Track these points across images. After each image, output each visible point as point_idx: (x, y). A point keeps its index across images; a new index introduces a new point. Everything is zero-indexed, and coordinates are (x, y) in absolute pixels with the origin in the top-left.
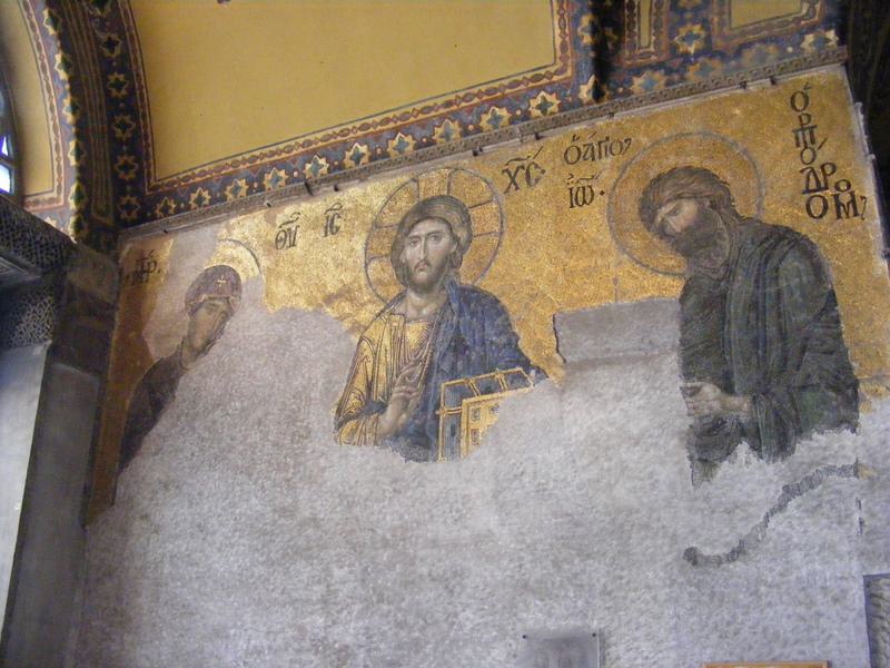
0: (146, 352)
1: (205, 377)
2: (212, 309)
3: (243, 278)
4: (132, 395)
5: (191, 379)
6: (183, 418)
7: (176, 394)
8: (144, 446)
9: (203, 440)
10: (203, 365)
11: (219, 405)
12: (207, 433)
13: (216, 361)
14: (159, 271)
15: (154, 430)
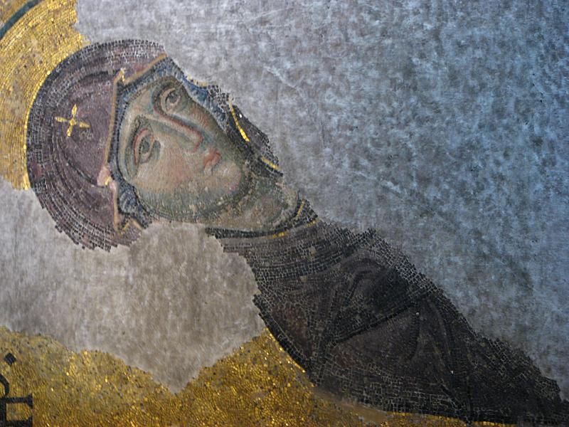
0: (222, 375)
1: (326, 133)
2: (142, 146)
3: (81, 40)
4: (348, 404)
5: (326, 182)
6: (432, 193)
7: (362, 228)
8: (498, 332)
9: (499, 112)
10: (292, 143)
11: (409, 71)
12: (480, 99)
13: (286, 101)
14: (10, 359)
15: (461, 296)
